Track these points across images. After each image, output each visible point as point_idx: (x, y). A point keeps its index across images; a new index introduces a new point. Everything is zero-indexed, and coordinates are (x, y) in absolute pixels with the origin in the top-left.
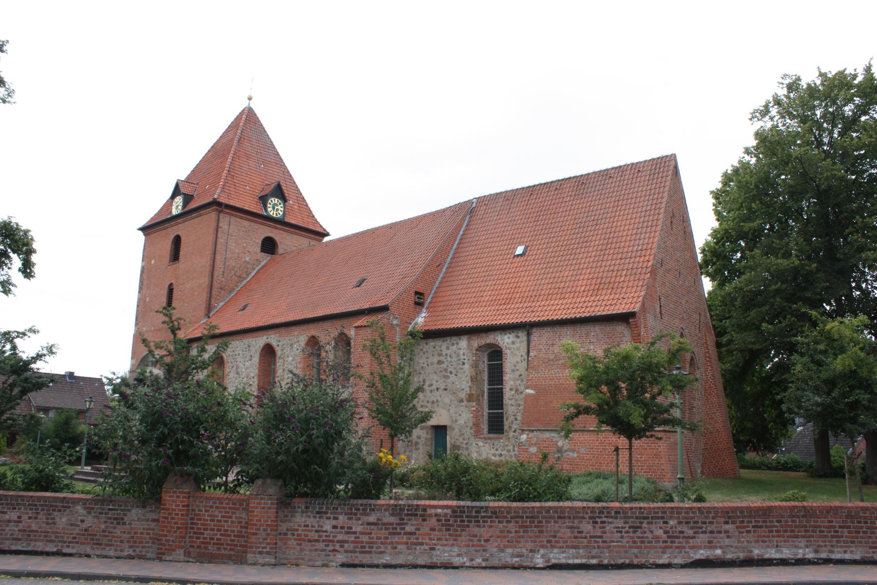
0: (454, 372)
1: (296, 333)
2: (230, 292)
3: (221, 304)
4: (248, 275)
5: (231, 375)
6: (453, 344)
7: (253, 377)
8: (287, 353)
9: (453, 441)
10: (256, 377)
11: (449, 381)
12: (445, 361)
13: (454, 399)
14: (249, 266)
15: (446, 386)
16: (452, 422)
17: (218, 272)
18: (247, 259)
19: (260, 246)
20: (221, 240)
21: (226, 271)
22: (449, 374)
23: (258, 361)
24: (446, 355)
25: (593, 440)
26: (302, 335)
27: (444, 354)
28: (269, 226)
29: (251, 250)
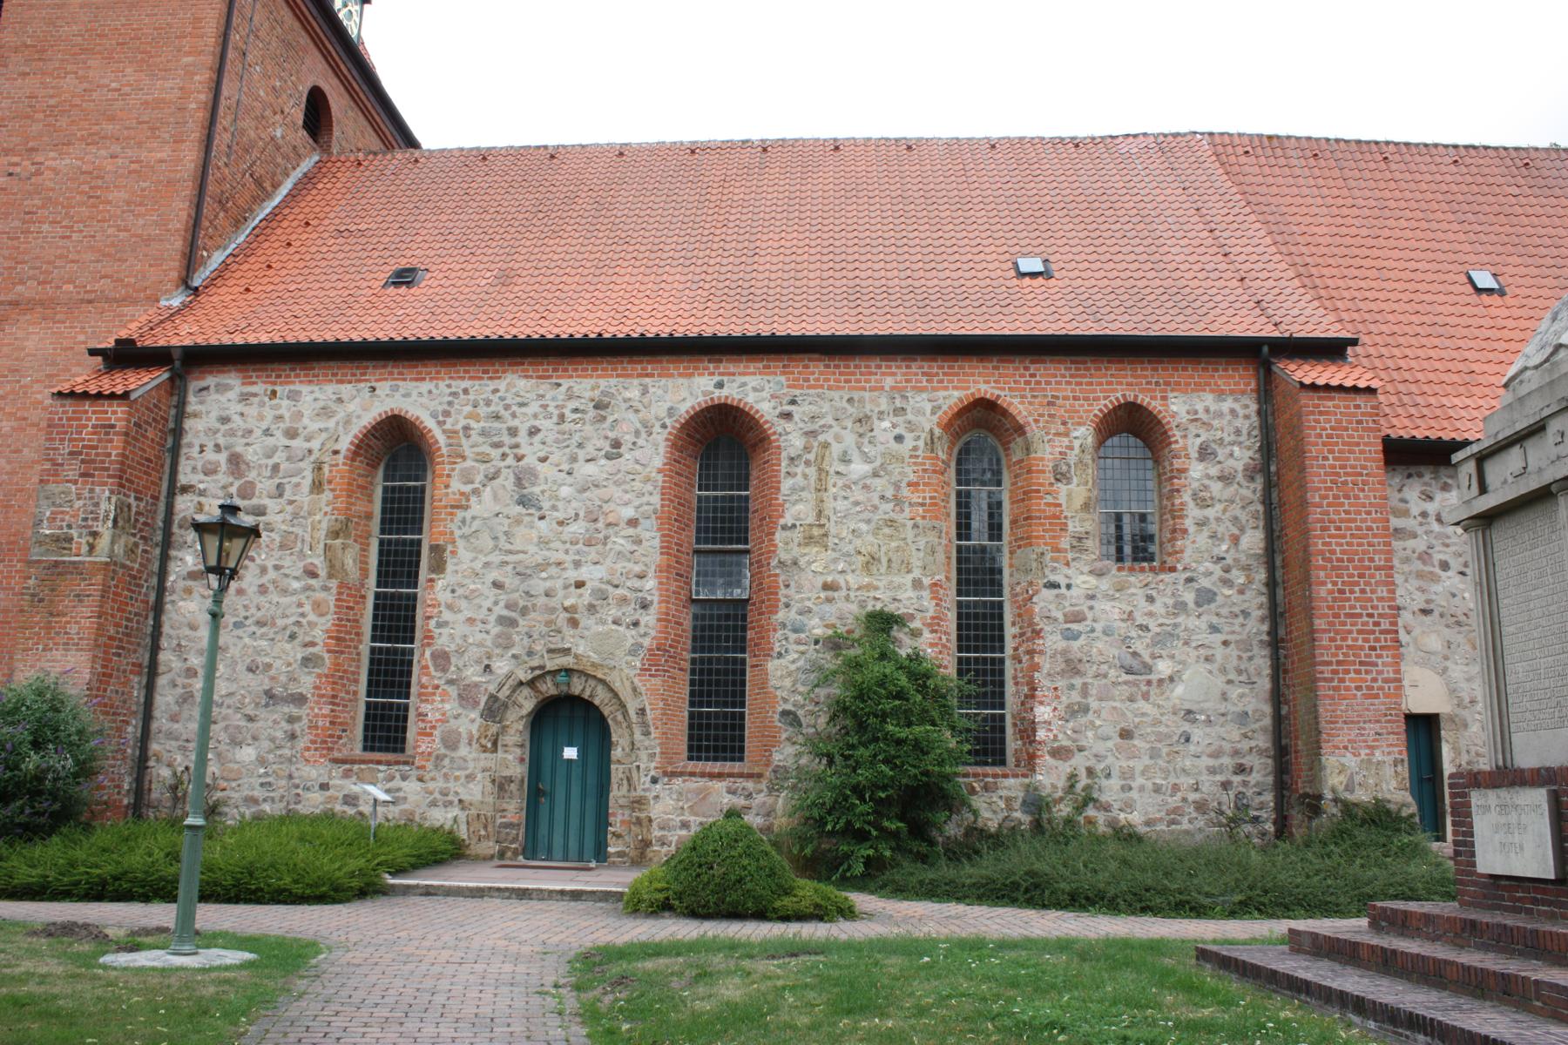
0: (1456, 564)
1: (889, 382)
2: (238, 223)
3: (217, 258)
4: (276, 186)
5: (483, 506)
6: (1445, 488)
7: (633, 523)
8: (836, 449)
9: (1464, 759)
10: (652, 523)
11: (1438, 588)
12: (1420, 530)
13: (1460, 638)
14: (279, 160)
15: (1428, 602)
17: (222, 140)
18: (279, 134)
19: (303, 106)
20: (235, 37)
21: (235, 148)
22: (1437, 570)
23: (658, 462)
24: (1424, 514)
26: (922, 390)
27: (1415, 511)
28: (326, 56)
29: (287, 110)
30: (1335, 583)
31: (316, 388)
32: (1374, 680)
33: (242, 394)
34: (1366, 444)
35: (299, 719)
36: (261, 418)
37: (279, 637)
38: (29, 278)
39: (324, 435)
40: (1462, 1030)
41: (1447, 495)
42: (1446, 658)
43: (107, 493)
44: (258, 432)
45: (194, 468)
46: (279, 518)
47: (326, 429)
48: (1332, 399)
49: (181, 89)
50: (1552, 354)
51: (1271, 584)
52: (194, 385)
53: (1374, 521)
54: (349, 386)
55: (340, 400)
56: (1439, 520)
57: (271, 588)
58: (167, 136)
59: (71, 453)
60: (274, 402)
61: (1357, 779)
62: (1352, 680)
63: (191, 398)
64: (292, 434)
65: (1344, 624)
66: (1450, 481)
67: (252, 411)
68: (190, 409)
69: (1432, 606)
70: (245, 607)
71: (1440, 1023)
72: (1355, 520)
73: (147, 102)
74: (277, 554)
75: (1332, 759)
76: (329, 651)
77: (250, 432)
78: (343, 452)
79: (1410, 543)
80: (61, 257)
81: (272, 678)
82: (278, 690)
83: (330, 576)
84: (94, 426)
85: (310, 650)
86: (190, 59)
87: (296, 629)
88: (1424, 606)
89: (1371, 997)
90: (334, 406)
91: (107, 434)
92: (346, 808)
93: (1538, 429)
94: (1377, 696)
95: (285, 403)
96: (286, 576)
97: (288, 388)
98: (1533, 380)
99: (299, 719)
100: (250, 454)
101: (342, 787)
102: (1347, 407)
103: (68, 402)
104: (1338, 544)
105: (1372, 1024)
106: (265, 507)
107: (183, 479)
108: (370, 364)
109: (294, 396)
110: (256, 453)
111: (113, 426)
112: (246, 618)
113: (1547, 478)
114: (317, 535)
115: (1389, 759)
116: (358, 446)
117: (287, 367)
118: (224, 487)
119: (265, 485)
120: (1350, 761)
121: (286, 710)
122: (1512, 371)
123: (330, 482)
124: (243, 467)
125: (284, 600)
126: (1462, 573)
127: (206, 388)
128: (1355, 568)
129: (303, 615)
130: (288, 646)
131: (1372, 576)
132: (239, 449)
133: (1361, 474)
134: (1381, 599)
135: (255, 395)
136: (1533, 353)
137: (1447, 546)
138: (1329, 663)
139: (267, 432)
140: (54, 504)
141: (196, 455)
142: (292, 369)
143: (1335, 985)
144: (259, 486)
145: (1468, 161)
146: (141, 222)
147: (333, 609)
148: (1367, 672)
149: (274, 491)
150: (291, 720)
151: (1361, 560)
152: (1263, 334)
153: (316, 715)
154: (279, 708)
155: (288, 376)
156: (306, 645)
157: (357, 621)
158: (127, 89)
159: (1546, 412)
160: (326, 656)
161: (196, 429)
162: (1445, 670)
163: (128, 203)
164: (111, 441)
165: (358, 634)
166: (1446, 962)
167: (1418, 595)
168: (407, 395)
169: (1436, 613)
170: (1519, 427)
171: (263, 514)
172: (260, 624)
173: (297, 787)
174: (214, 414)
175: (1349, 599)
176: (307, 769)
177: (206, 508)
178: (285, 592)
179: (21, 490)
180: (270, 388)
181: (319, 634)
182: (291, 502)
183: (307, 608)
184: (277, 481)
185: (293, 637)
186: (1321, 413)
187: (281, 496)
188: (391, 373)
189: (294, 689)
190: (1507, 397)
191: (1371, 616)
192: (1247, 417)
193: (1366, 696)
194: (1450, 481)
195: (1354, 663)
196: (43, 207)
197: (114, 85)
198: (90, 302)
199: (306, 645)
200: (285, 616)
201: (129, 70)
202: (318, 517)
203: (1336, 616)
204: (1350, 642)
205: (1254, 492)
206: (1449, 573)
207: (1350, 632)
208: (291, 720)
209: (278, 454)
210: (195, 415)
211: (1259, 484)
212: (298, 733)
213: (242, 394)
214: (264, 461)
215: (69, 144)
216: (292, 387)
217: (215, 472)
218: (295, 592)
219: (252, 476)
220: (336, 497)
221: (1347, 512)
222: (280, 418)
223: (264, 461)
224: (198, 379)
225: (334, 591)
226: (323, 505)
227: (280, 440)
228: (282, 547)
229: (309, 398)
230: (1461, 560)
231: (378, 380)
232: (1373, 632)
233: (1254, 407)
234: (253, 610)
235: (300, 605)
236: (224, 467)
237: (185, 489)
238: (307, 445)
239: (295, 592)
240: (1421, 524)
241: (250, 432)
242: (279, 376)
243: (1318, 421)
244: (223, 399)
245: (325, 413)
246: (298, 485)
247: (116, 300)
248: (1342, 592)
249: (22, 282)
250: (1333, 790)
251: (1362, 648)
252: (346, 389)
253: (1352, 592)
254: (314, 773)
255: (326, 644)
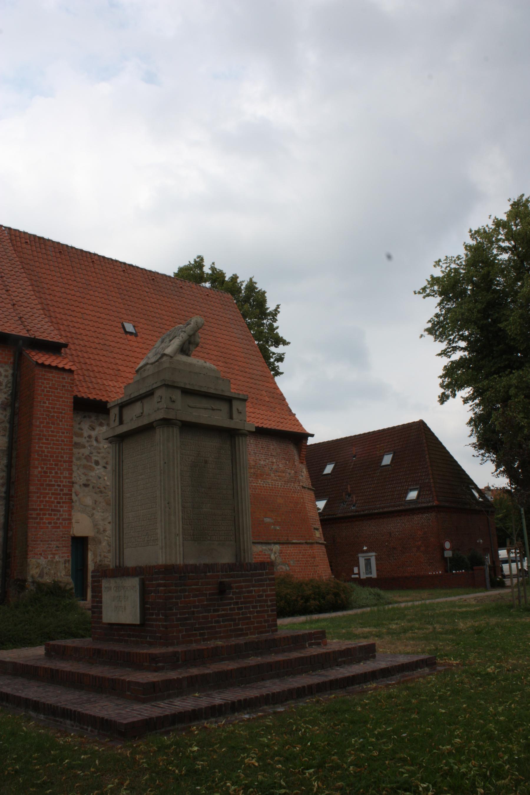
0: (102, 462)
6: (101, 425)
9: (99, 558)
11: (93, 474)
12: (87, 445)
15: (88, 480)
16: (98, 532)
22: (93, 465)
24: (90, 437)
25: (297, 553)
30: (42, 468)
32: (58, 519)
34: (66, 398)
40: (90, 715)
41: (101, 428)
42: (94, 509)
48: (52, 373)
50: (160, 358)
51: (9, 466)
53: (65, 437)
56: (97, 440)
61: (45, 571)
62: (47, 519)
65: (45, 489)
66: (103, 422)
69: (89, 483)
71: (79, 712)
72: (56, 436)
75: (33, 560)
79: (82, 451)
88: (85, 482)
89: (43, 700)
93: (150, 394)
94: (59, 527)
98: (150, 370)
102: (59, 378)
104: (46, 448)
105: (42, 717)
113: (152, 418)
115: (62, 560)
120: (42, 561)
122: (142, 363)
126: (105, 467)
128: (54, 461)
131: (62, 465)
133: (61, 413)
134: (65, 477)
136: (151, 357)
137: (99, 453)
138: (36, 510)
143: (23, 694)
145: (129, 271)
148: (55, 515)
151: (57, 457)
152: (21, 334)
159: (154, 386)
162: (93, 515)
166: (84, 675)
167: (83, 477)
169: (91, 486)
170: (142, 392)
175: (49, 477)
186: (45, 379)
190: (137, 377)
191: (59, 486)
192: (6, 376)
193: (53, 527)
194: (103, 422)
195: (48, 510)
203: (42, 485)
204: (47, 499)
205: (5, 416)
206: (99, 467)
207: (48, 494)
211: (8, 413)
221: (52, 432)
230: (105, 461)
232: (60, 494)
233: (11, 372)
240: (88, 441)
243: (43, 383)
248: (45, 472)
250: (33, 577)
251: (53, 502)
253: (51, 473)
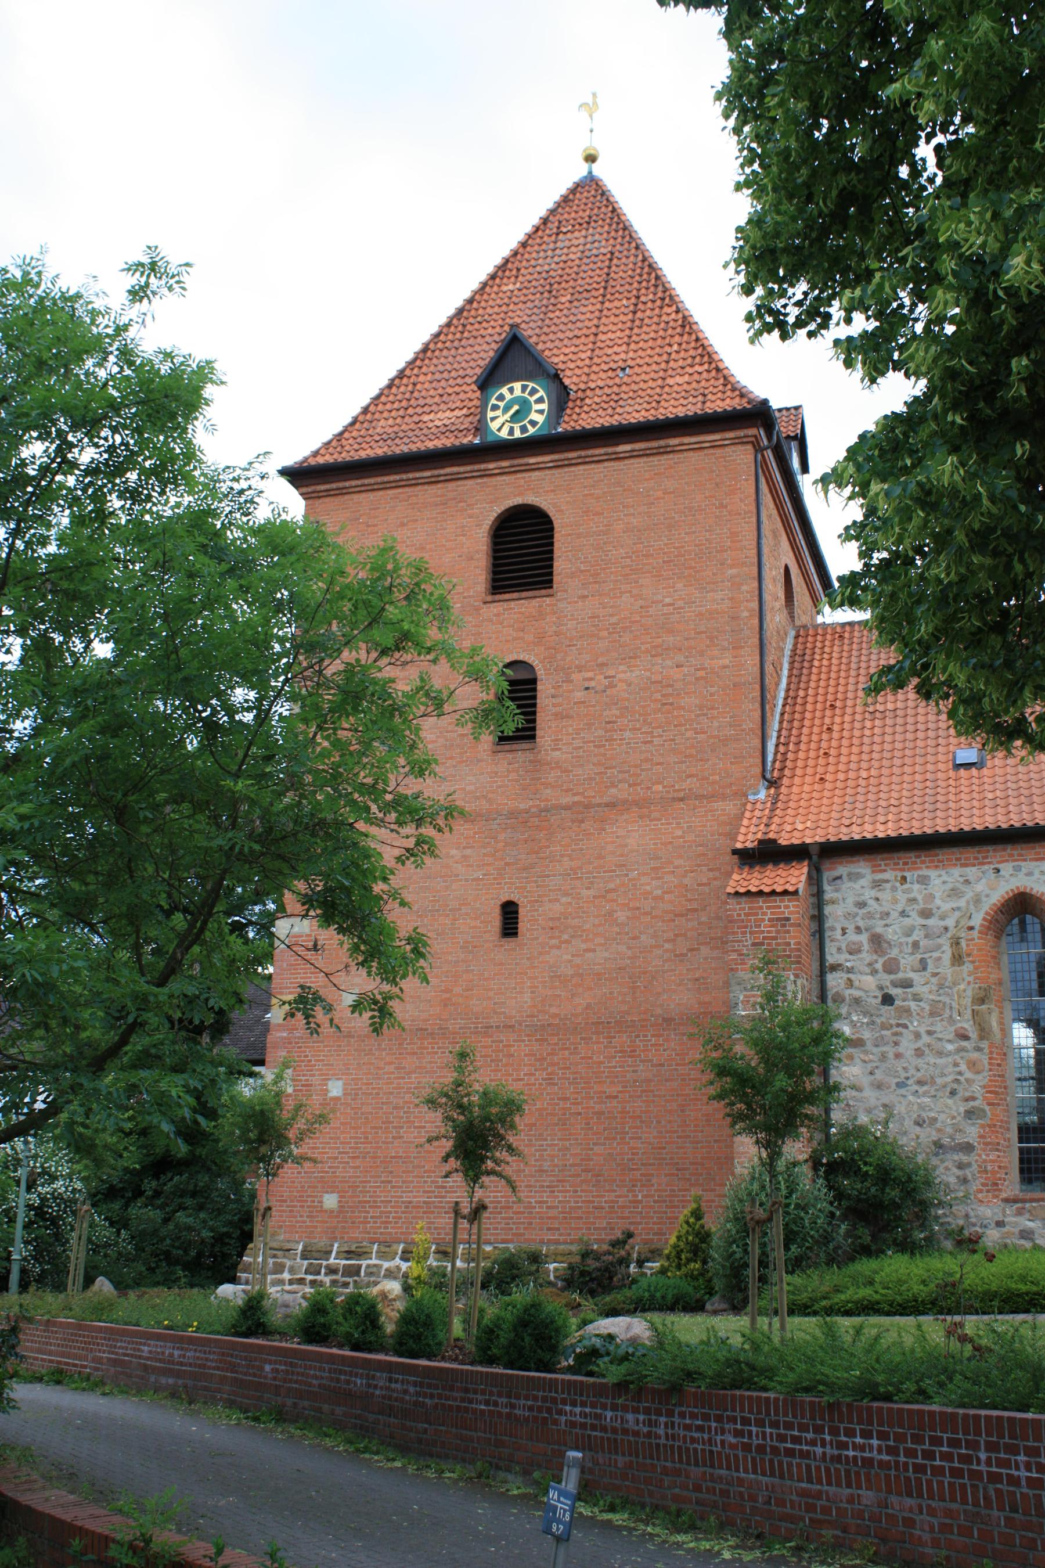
31: (943, 873)
33: (874, 881)
35: (969, 1165)
36: (895, 901)
37: (939, 1094)
38: (620, 781)
39: (957, 914)
43: (792, 977)
44: (894, 915)
45: (839, 949)
46: (925, 989)
47: (959, 909)
49: (731, 599)
52: (827, 875)
54: (974, 869)
55: (967, 882)
57: (927, 1051)
58: (726, 643)
59: (754, 944)
60: (905, 886)
63: (827, 887)
64: (926, 914)
67: (886, 895)
68: (827, 896)
70: (904, 1068)
73: (700, 614)
74: (928, 1021)
76: (989, 1104)
77: (888, 914)
78: (977, 927)
80: (646, 760)
81: (939, 1130)
82: (946, 1141)
83: (981, 1038)
84: (770, 920)
85: (972, 1103)
86: (734, 571)
87: (955, 1086)
90: (963, 888)
91: (784, 926)
92: (1022, 1242)
95: (916, 887)
96: (940, 1039)
97: (916, 873)
99: (969, 1165)
100: (890, 934)
101: (1016, 1224)
103: (744, 899)
106: (912, 981)
107: (830, 959)
108: (990, 848)
109: (924, 880)
110: (896, 933)
111: (788, 919)
112: (907, 1078)
114: (964, 1002)
116: (990, 922)
117: (912, 855)
118: (870, 964)
119: (908, 961)
121: (956, 1157)
123: (968, 955)
124: (885, 945)
125: (939, 1061)
127: (840, 878)
129: (960, 1073)
130: (950, 1102)
132: (879, 930)
135: (887, 881)
139: (903, 914)
140: (745, 989)
141: (839, 937)
142: (917, 857)
144: (902, 961)
146: (716, 724)
147: (987, 1067)
149: (917, 966)
150: (961, 1166)
153: (985, 1161)
154: (948, 1156)
155: (915, 863)
156: (967, 1100)
157: (1003, 1076)
158: (681, 603)
160: (987, 1108)
161: (835, 914)
163: (701, 708)
164: (788, 932)
165: (1005, 1088)
168: (1030, 874)
171: (911, 986)
172: (920, 1083)
173: (974, 1225)
174: (850, 900)
176: (982, 1209)
177: (856, 983)
178: (940, 1054)
179: (645, 973)
180: (900, 874)
181: (977, 1089)
182: (935, 975)
183: (963, 1067)
184: (919, 956)
185: (953, 1093)
187: (924, 969)
188: (1012, 855)
189: (960, 1139)
196: (622, 716)
197: (667, 600)
198: (682, 800)
199: (967, 1100)
200: (943, 1075)
201: (679, 586)
202: (962, 987)
208: (961, 1166)
209: (916, 932)
210: (833, 902)
212: (970, 1177)
213: (874, 881)
214: (903, 940)
215: (635, 657)
216: (920, 873)
217: (859, 951)
218: (949, 1054)
219: (894, 953)
220: (976, 968)
222: (914, 900)
223: (903, 940)
224: (830, 869)
225: (986, 1051)
226: (965, 975)
227: (916, 920)
228: (932, 1014)
229: (938, 881)
231: (999, 862)
234: (912, 1071)
235: (956, 1065)
236: (866, 947)
237: (834, 968)
238: (942, 923)
239: (949, 1054)
241: (888, 914)
242: (906, 864)
244: (857, 886)
245: (954, 893)
246: (939, 959)
247: (703, 796)
249: (613, 785)
252: (971, 872)
254: (988, 1212)
255: (985, 1098)
